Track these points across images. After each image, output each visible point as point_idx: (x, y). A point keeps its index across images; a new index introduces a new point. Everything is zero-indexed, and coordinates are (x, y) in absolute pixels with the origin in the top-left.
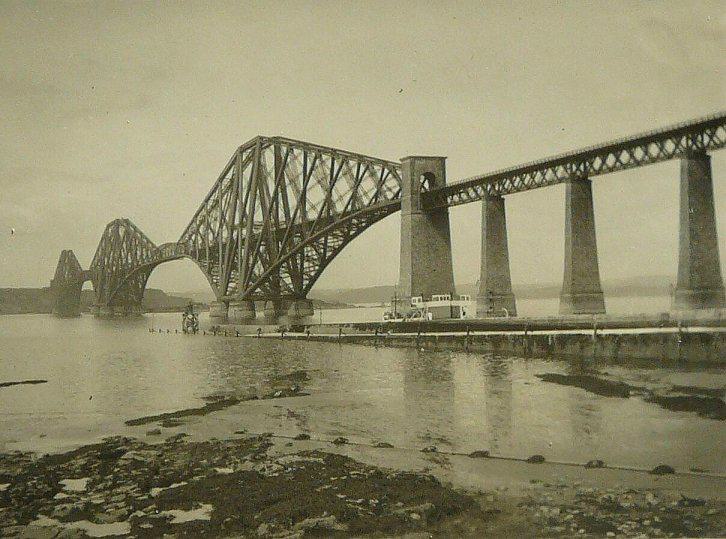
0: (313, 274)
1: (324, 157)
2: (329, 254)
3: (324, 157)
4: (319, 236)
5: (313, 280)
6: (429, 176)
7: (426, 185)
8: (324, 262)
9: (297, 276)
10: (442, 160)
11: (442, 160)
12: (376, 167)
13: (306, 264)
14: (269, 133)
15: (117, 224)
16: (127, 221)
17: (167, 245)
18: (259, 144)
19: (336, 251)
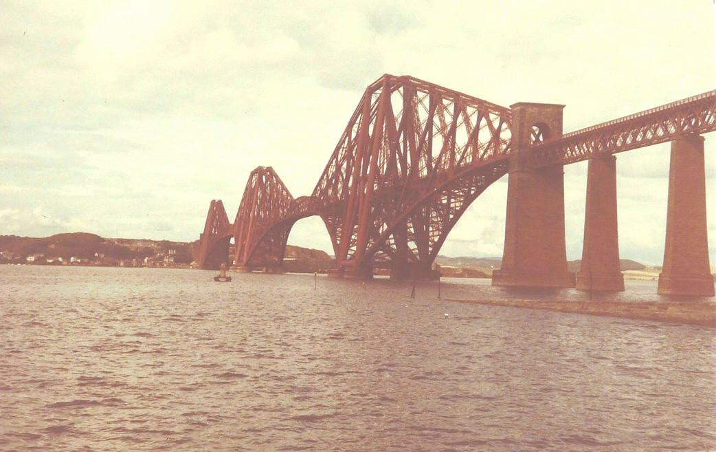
0: (436, 239)
1: (445, 102)
2: (451, 216)
3: (445, 102)
4: (439, 193)
5: (438, 246)
6: (544, 129)
7: (541, 138)
8: (447, 226)
9: (422, 239)
10: (558, 110)
11: (559, 108)
12: (492, 116)
13: (431, 229)
14: (397, 73)
15: (259, 172)
16: (270, 169)
17: (303, 199)
18: (388, 83)
19: (458, 214)
